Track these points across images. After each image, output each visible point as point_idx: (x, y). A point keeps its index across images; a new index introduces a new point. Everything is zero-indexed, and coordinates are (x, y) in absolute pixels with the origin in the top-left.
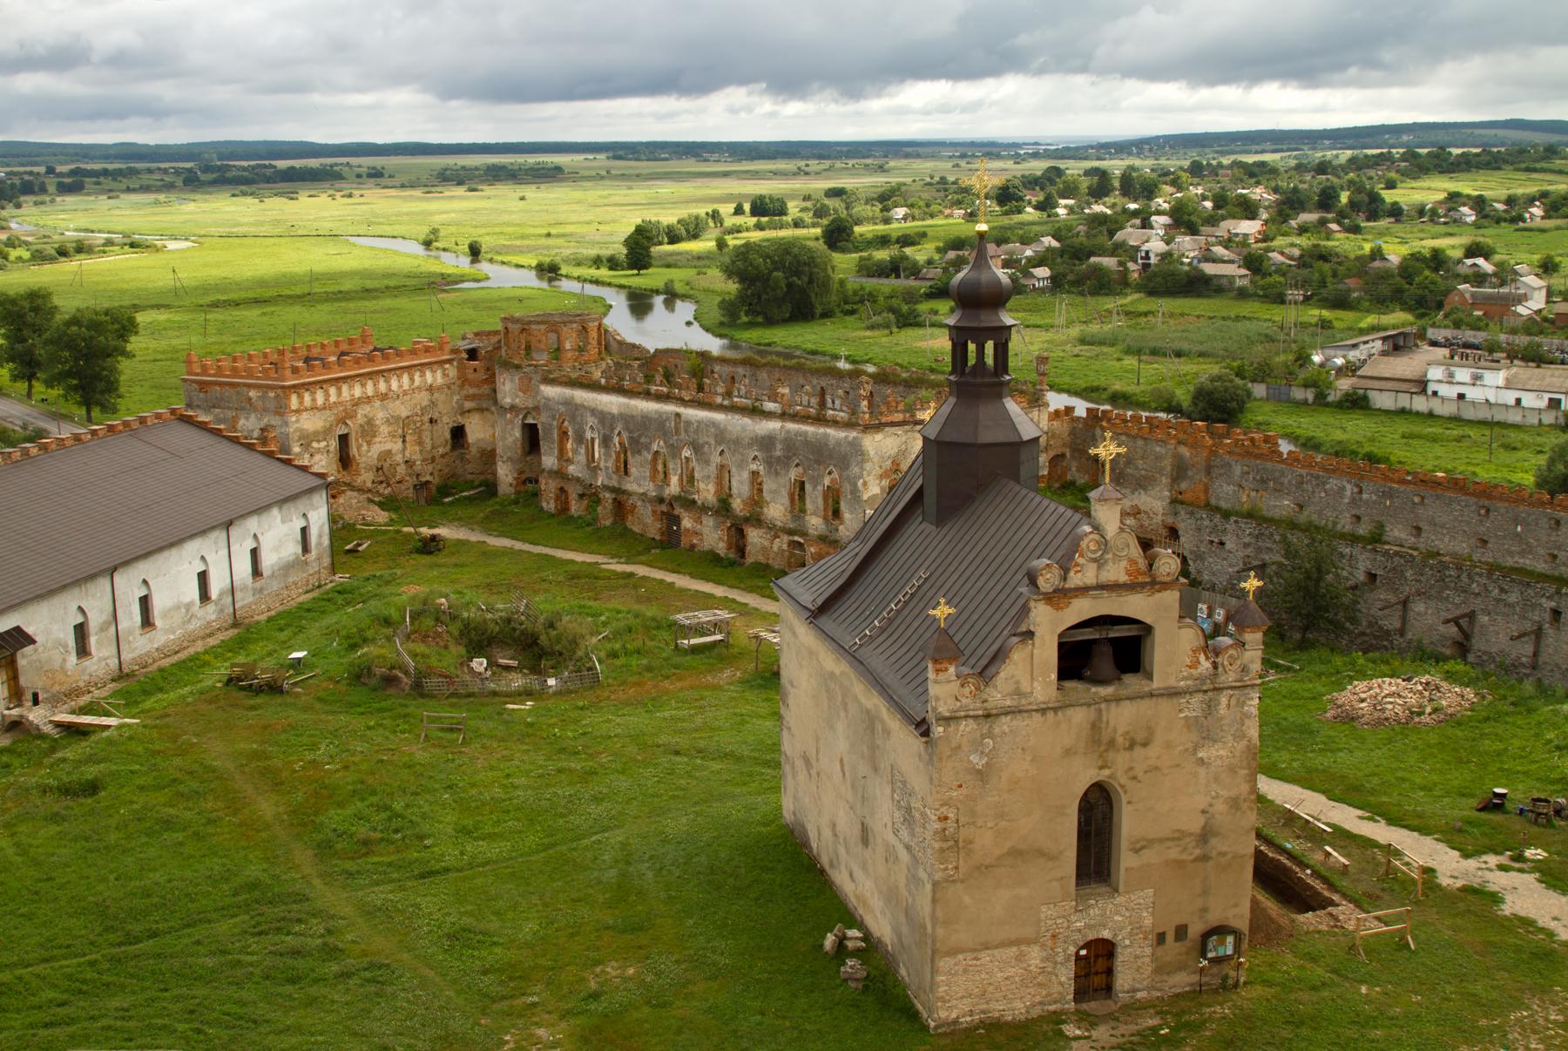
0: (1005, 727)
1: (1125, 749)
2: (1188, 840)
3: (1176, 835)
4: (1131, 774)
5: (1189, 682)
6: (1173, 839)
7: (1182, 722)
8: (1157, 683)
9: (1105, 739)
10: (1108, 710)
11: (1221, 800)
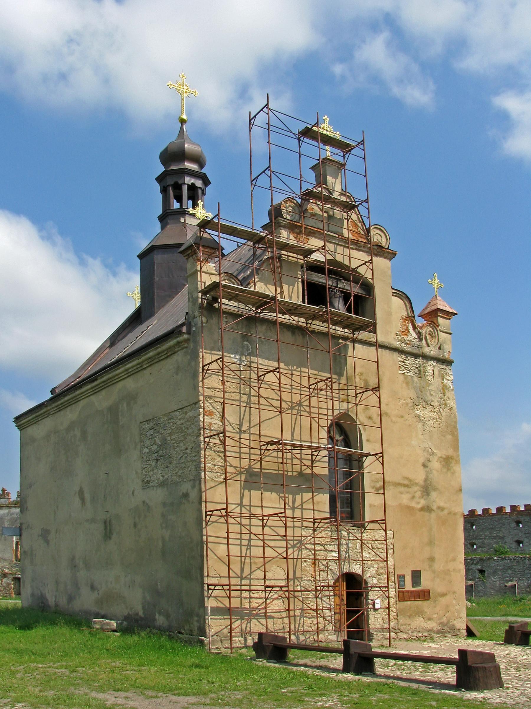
8: (381, 338)
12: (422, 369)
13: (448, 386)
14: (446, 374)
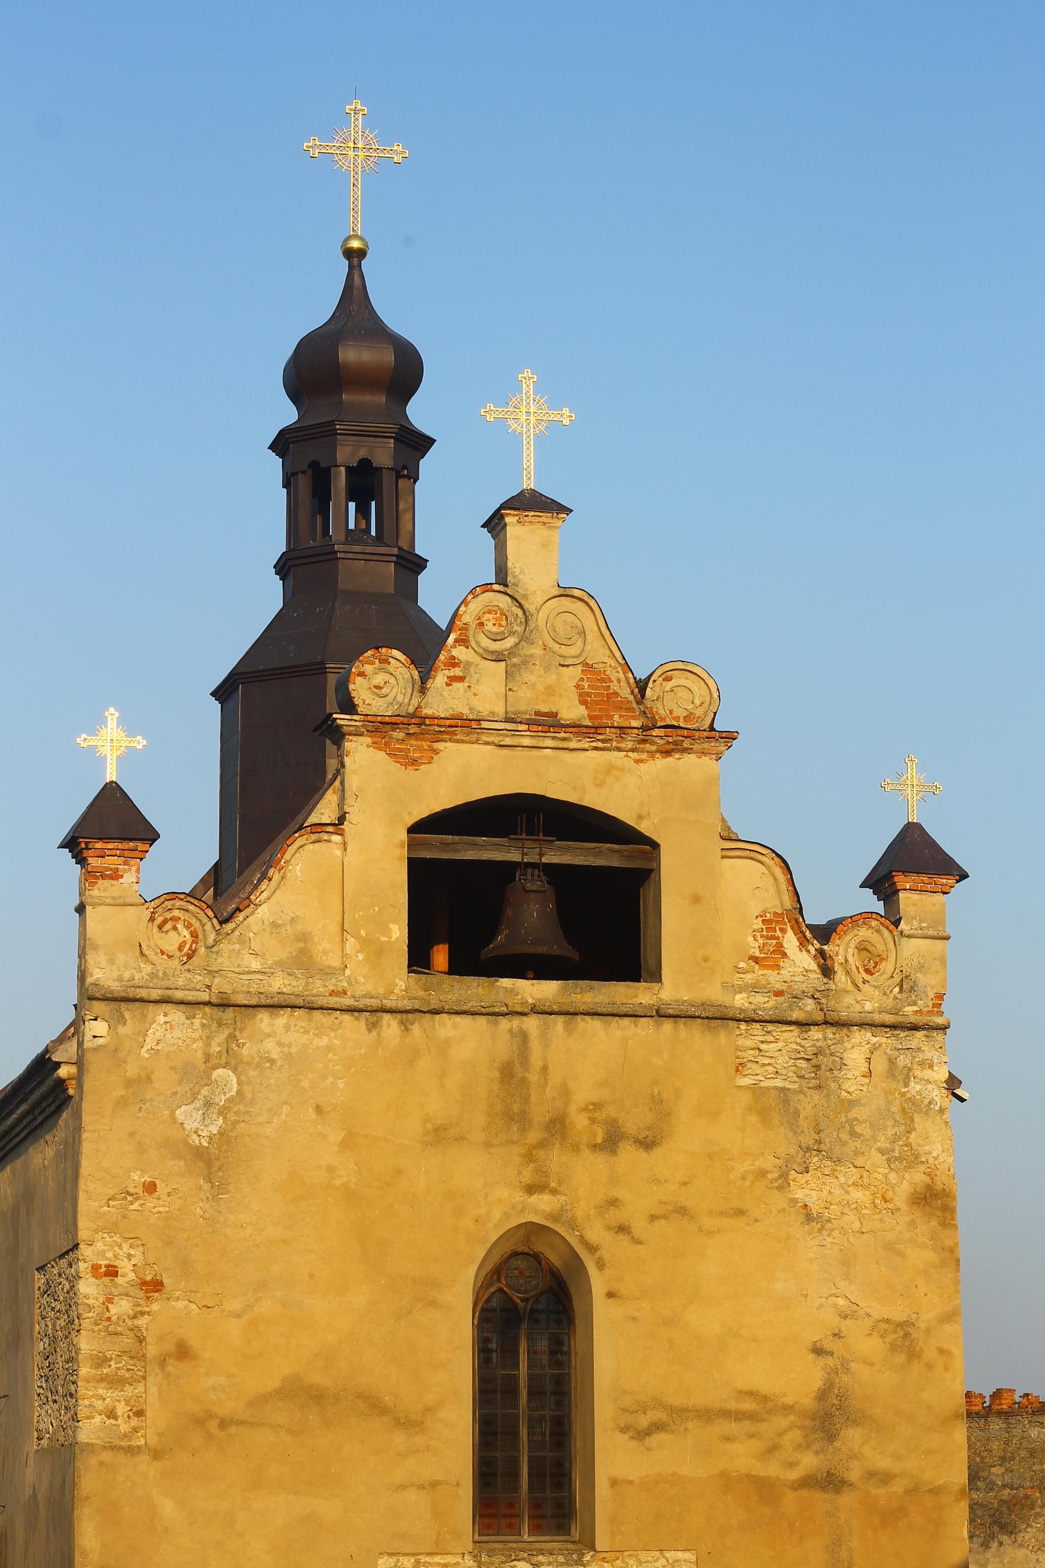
0: (269, 1045)
1: (594, 1147)
2: (783, 1422)
3: (748, 1405)
4: (614, 1216)
5: (759, 999)
6: (740, 1416)
7: (746, 1098)
9: (539, 1114)
10: (544, 1035)
11: (869, 1323)
12: (823, 1061)
13: (926, 1101)
14: (922, 1064)
